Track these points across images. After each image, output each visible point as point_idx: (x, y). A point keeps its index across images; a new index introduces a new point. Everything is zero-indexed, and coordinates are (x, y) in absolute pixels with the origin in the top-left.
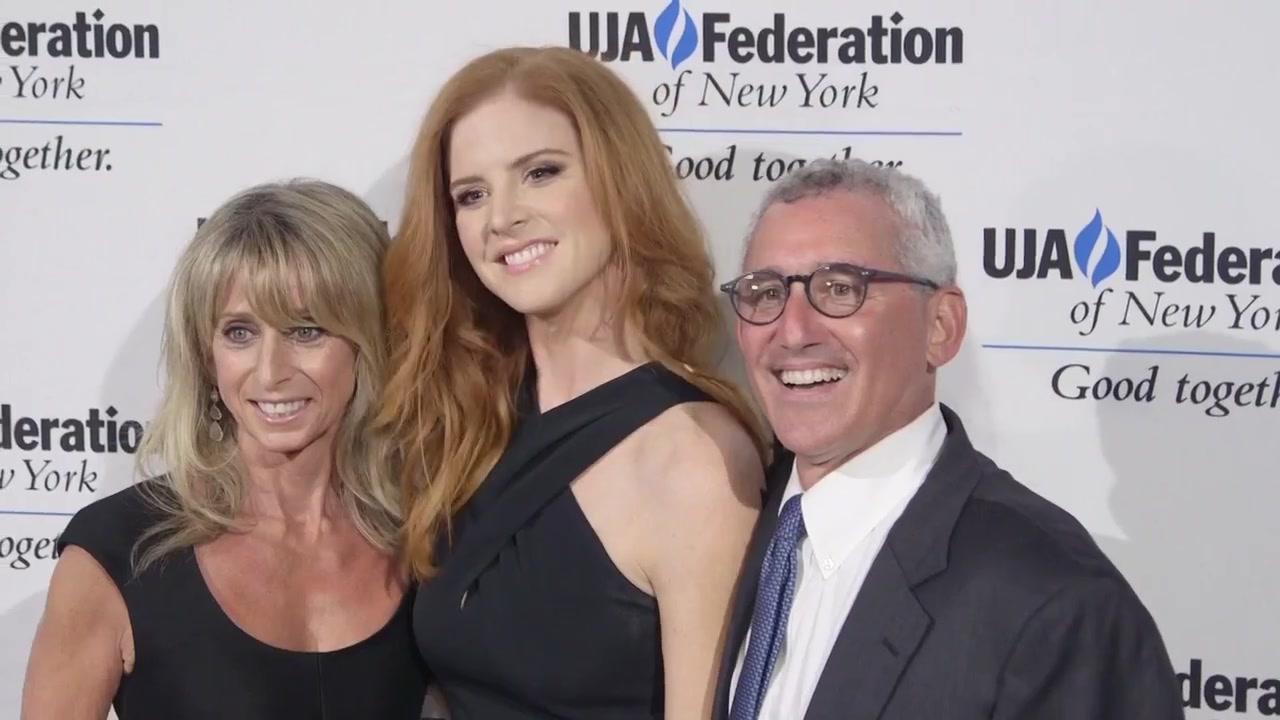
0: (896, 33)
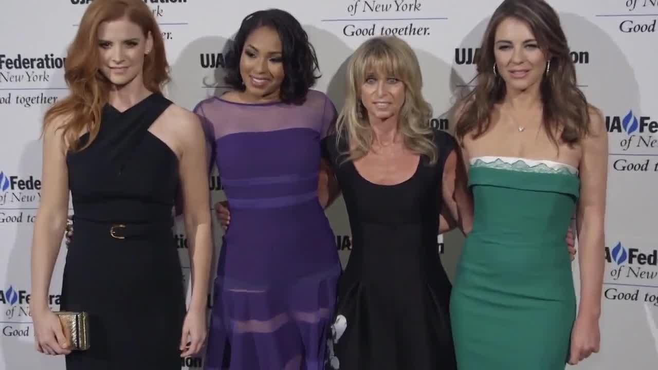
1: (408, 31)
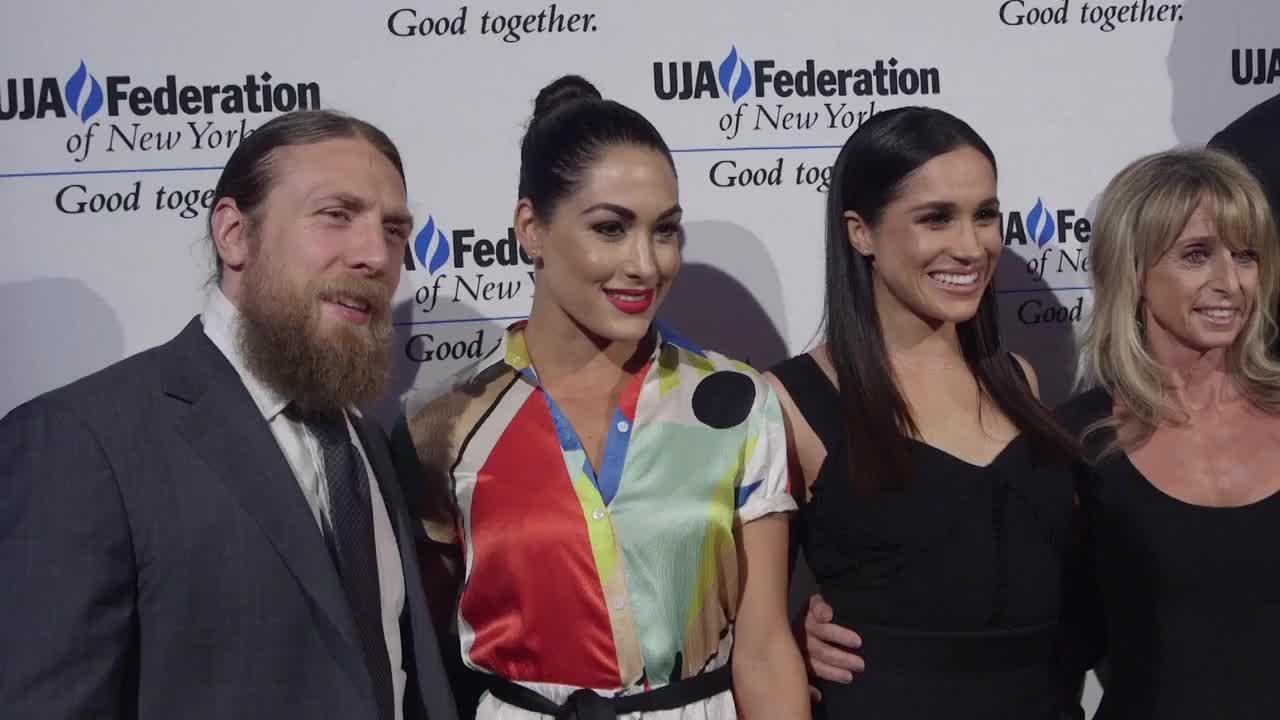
0: (267, 89)
1: (546, 22)
